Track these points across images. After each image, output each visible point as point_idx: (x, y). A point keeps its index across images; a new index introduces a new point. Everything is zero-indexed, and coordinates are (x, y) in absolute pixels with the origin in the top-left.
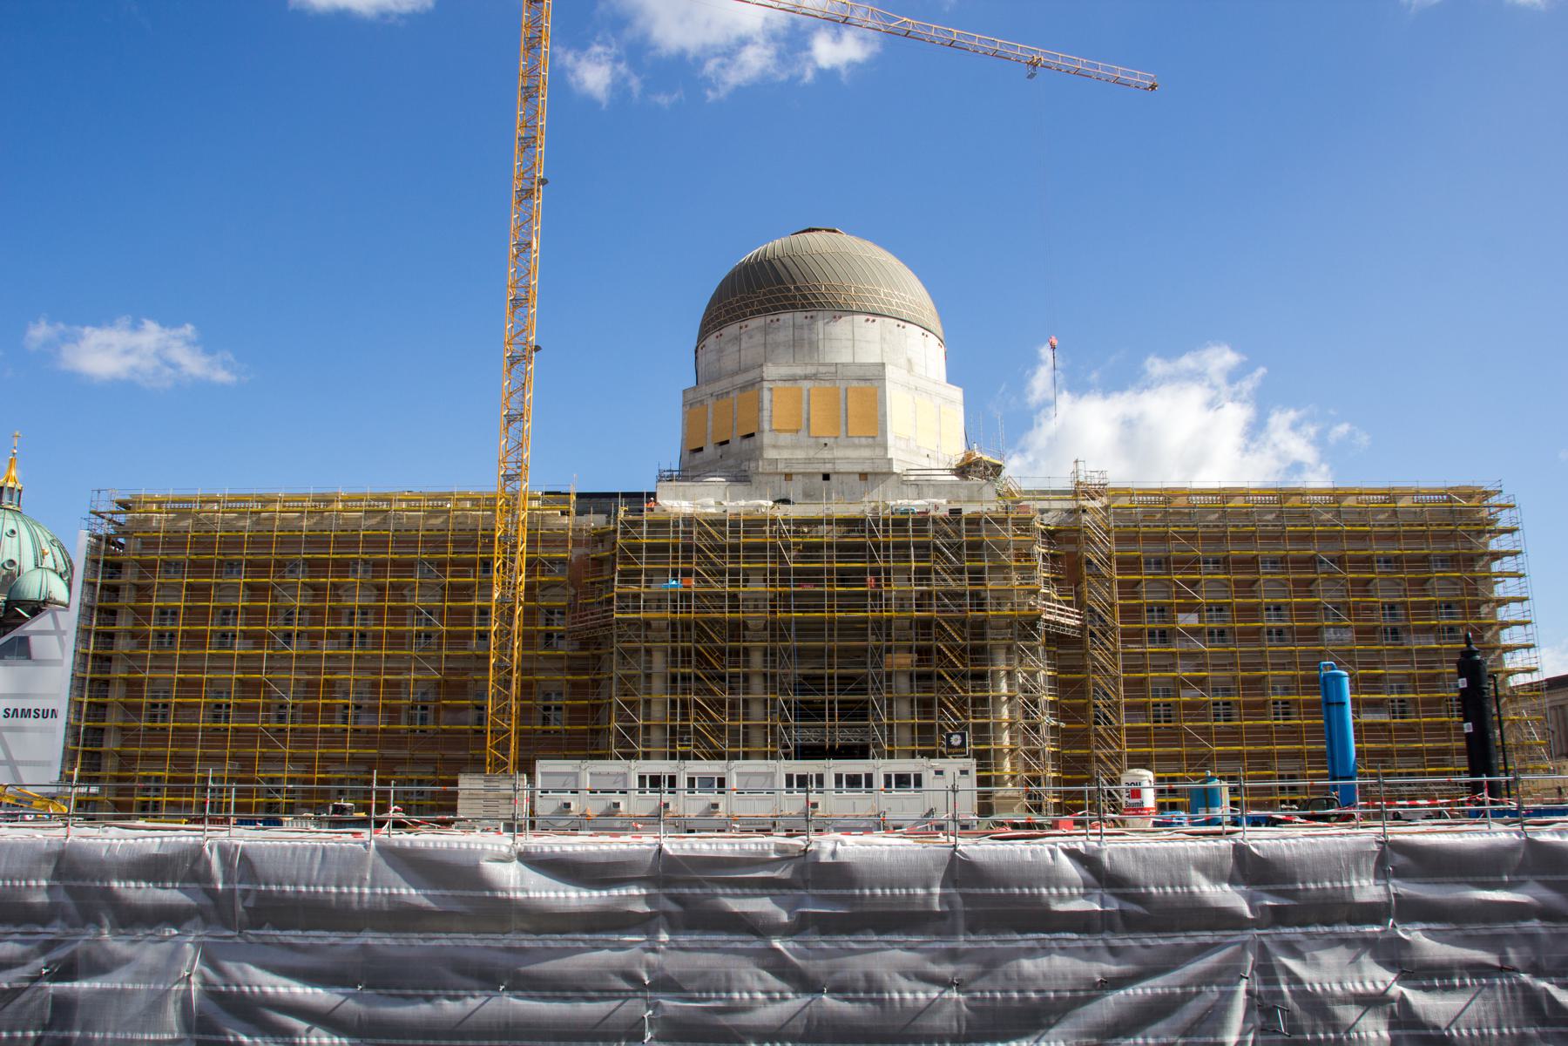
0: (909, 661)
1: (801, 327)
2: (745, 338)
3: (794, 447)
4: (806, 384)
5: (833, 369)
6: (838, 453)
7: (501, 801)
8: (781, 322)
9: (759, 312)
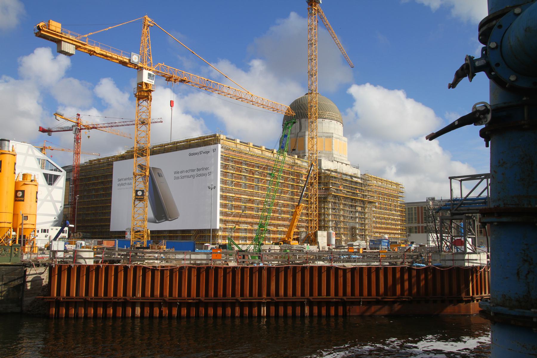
2: (324, 123)
6: (342, 158)
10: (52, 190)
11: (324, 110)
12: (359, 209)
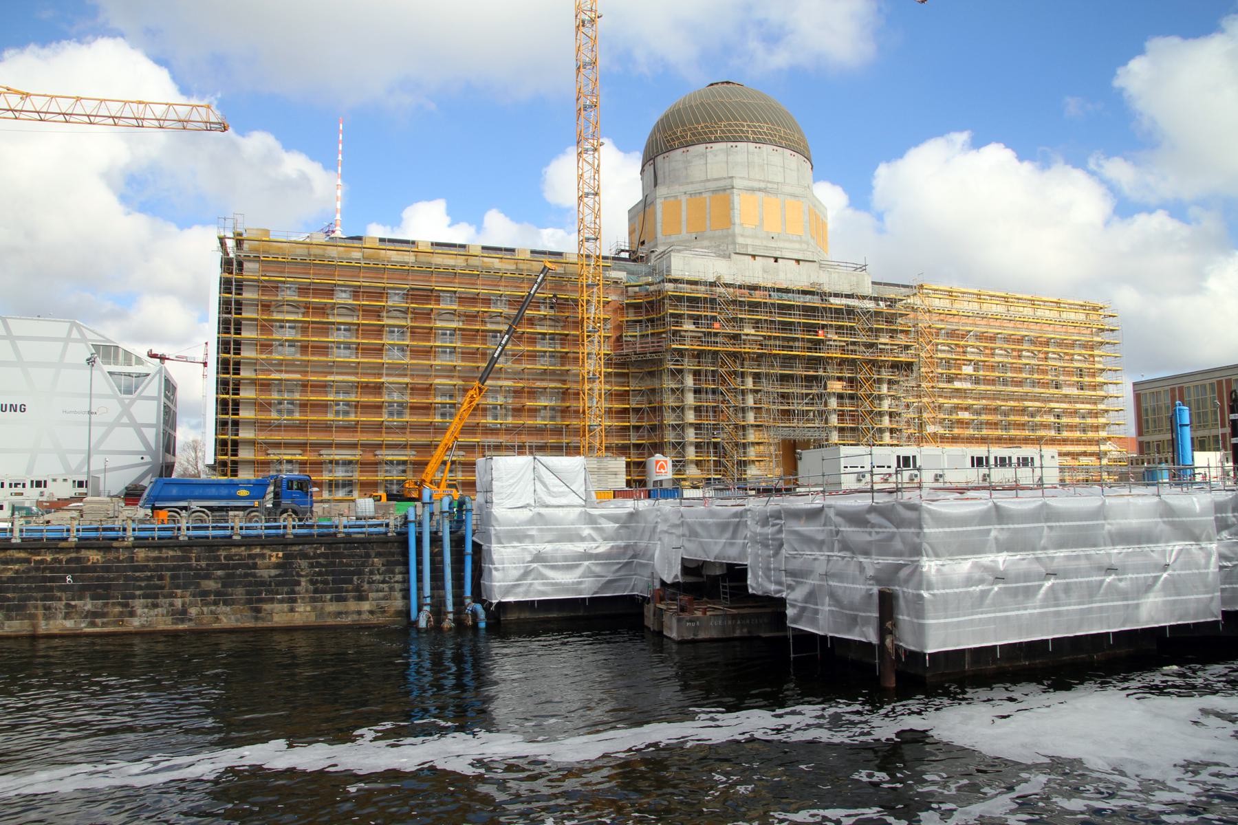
0: (840, 387)
1: (753, 154)
2: (710, 156)
5: (775, 186)
6: (781, 244)
7: (610, 476)
8: (738, 148)
12: (836, 387)
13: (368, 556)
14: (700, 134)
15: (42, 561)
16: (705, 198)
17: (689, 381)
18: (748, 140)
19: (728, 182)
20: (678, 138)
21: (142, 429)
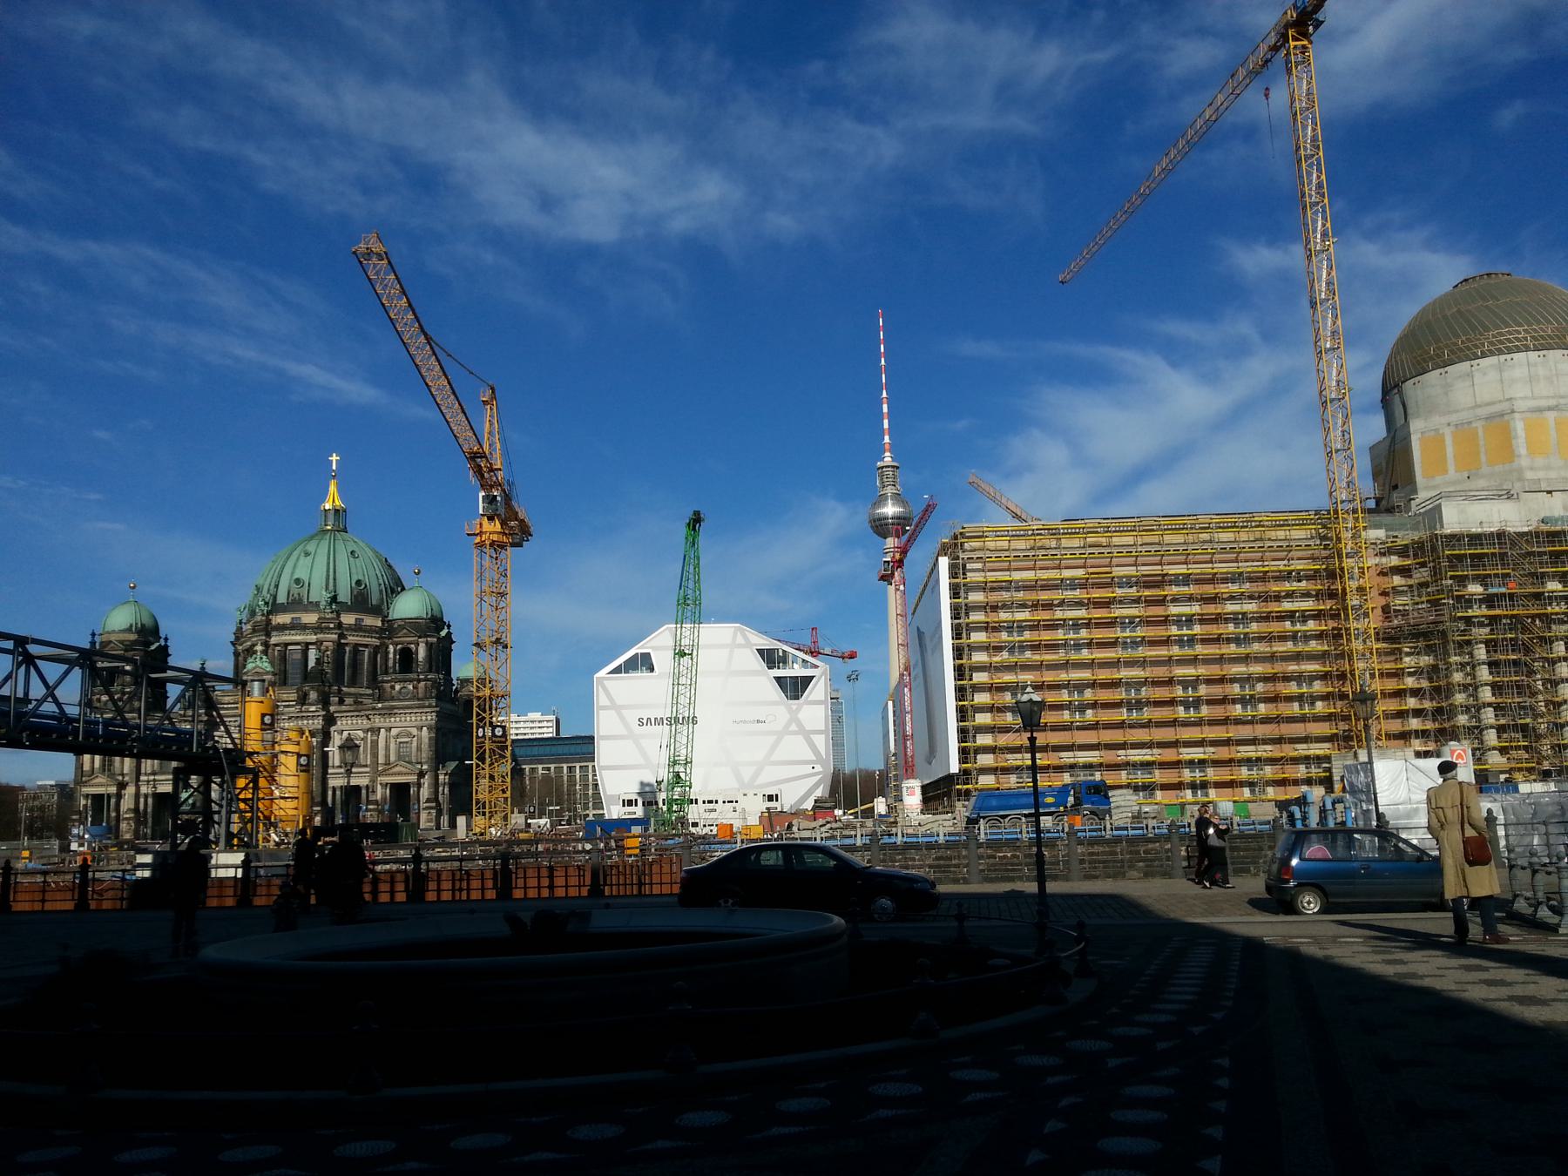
1: (1535, 365)
2: (1478, 378)
3: (1548, 468)
4: (1551, 415)
9: (1492, 354)
10: (798, 710)
11: (1474, 329)
13: (1261, 849)
14: (1461, 350)
15: (1005, 857)
16: (1477, 427)
17: (1481, 653)
18: (1527, 349)
19: (1505, 406)
20: (1431, 358)
21: (812, 736)
